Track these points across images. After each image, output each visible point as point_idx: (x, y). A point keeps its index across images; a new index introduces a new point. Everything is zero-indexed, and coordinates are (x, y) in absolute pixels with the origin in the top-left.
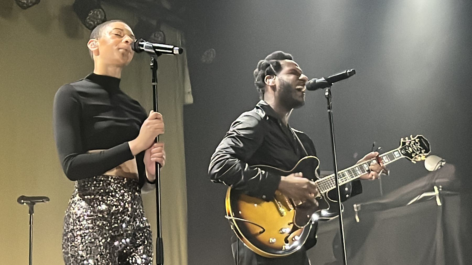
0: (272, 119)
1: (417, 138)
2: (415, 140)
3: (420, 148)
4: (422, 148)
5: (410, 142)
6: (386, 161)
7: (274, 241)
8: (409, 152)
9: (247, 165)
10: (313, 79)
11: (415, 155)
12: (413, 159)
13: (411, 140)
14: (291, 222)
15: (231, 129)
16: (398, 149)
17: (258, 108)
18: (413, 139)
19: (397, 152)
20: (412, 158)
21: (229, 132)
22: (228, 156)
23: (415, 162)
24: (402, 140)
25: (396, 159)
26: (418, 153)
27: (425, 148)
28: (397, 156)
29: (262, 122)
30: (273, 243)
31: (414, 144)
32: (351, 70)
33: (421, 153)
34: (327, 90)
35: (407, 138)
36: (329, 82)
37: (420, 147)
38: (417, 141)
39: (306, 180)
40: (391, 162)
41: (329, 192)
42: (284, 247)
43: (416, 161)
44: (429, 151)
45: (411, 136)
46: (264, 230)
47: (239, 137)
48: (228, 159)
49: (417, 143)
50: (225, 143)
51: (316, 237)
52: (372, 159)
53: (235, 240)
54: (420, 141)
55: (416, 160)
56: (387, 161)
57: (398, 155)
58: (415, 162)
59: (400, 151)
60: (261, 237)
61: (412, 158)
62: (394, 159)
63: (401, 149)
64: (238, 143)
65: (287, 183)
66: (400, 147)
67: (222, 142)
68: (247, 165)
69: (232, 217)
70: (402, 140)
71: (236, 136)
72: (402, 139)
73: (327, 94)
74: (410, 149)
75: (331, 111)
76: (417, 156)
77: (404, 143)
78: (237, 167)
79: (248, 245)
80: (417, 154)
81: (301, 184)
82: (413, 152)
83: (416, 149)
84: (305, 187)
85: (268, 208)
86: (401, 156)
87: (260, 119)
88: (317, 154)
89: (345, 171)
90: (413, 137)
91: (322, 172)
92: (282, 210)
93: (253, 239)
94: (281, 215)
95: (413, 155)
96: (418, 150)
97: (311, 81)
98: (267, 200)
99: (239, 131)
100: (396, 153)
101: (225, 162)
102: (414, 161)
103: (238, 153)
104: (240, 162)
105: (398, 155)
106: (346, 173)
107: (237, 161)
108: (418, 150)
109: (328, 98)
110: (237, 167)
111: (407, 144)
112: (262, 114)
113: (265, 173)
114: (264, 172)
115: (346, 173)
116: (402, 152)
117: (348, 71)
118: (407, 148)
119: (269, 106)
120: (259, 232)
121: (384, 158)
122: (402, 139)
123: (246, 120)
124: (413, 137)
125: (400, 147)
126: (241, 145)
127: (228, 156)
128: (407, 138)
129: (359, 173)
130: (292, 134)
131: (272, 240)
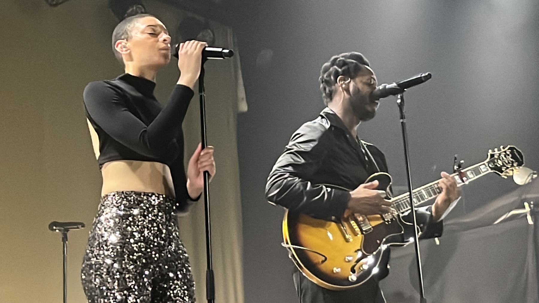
0: (337, 130)
1: (509, 149)
2: (505, 152)
3: (512, 161)
4: (514, 160)
5: (500, 154)
6: (472, 177)
7: (338, 270)
8: (499, 166)
10: (383, 85)
11: (506, 169)
12: (504, 174)
13: (501, 153)
14: (359, 248)
15: (291, 143)
16: (485, 162)
18: (503, 150)
19: (484, 166)
20: (502, 172)
21: (288, 147)
23: (506, 177)
24: (490, 152)
25: (482, 174)
26: (509, 166)
27: (517, 160)
28: (483, 170)
29: (326, 134)
30: (337, 273)
31: (505, 157)
32: (427, 74)
33: (512, 166)
34: (399, 96)
35: (496, 150)
36: (402, 88)
37: (511, 159)
38: (508, 153)
40: (476, 177)
42: (350, 277)
43: (507, 176)
44: (523, 163)
45: (502, 147)
46: (326, 259)
48: (286, 178)
49: (508, 155)
50: (284, 159)
52: (454, 174)
53: (296, 270)
55: (507, 174)
56: (471, 176)
57: (485, 169)
58: (506, 177)
59: (487, 164)
60: (324, 267)
61: (502, 172)
62: (480, 173)
63: (489, 163)
64: (298, 160)
66: (488, 160)
67: (280, 159)
69: (290, 245)
70: (490, 152)
71: (295, 151)
72: (490, 151)
73: (399, 101)
74: (500, 162)
75: (405, 121)
76: (507, 170)
77: (492, 156)
78: (297, 187)
79: (307, 273)
80: (508, 168)
82: (504, 166)
83: (507, 162)
86: (488, 170)
88: (389, 169)
89: (422, 189)
90: (504, 148)
94: (347, 241)
95: (503, 169)
96: (509, 163)
97: (381, 87)
99: (300, 145)
100: (482, 167)
101: (283, 182)
102: (505, 175)
103: (297, 170)
104: (301, 181)
105: (485, 169)
106: (424, 192)
107: (297, 180)
108: (509, 163)
109: (401, 106)
110: (297, 187)
111: (496, 157)
115: (424, 192)
116: (490, 165)
117: (423, 75)
118: (496, 161)
120: (320, 261)
121: (468, 173)
122: (490, 151)
124: (504, 148)
125: (488, 160)
128: (496, 150)
130: (358, 146)
131: (336, 270)
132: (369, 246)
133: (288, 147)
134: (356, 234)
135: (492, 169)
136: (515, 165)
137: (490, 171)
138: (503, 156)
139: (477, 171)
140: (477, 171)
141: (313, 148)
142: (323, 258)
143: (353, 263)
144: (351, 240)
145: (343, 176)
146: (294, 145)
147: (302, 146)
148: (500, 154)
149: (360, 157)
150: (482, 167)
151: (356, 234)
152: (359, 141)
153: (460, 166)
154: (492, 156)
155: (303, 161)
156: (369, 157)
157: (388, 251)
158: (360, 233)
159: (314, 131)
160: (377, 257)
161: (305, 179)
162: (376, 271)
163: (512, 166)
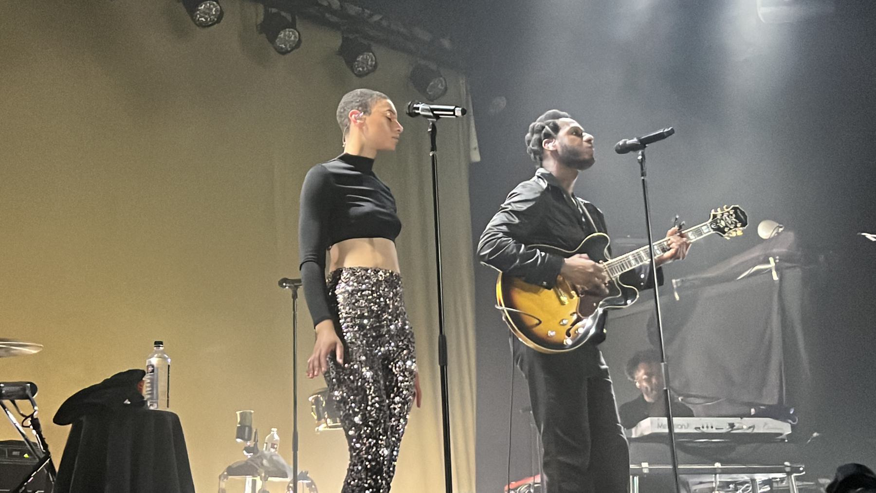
0: (555, 190)
5: (723, 214)
6: (693, 238)
9: (523, 246)
13: (724, 213)
15: (506, 202)
17: (539, 177)
20: (724, 233)
21: (503, 205)
22: (501, 235)
24: (713, 212)
29: (544, 192)
33: (736, 227)
35: (719, 209)
39: (592, 262)
41: (621, 276)
47: (516, 213)
50: (498, 218)
51: (605, 331)
54: (735, 213)
57: (707, 230)
61: (724, 233)
63: (711, 224)
65: (571, 267)
66: (710, 220)
67: (494, 218)
68: (523, 246)
70: (713, 212)
77: (715, 216)
78: (510, 248)
81: (585, 267)
84: (591, 270)
85: (549, 295)
87: (541, 190)
91: (614, 251)
92: (564, 298)
93: (528, 332)
95: (726, 230)
98: (548, 288)
100: (704, 228)
107: (511, 241)
110: (510, 248)
111: (719, 217)
112: (544, 185)
113: (545, 256)
114: (543, 254)
119: (550, 174)
123: (527, 191)
125: (710, 220)
126: (517, 221)
127: (501, 235)
128: (719, 209)
129: (658, 252)
132: (584, 310)
133: (503, 205)
134: (571, 297)
135: (714, 230)
136: (739, 225)
137: (712, 232)
138: (725, 215)
139: (699, 232)
140: (699, 232)
141: (529, 209)
142: (537, 322)
143: (569, 327)
144: (567, 303)
145: (559, 236)
146: (509, 204)
147: (518, 205)
148: (723, 214)
149: (574, 216)
150: (704, 228)
151: (571, 297)
152: (575, 199)
153: (680, 227)
154: (715, 216)
155: (517, 221)
156: (586, 218)
157: (605, 312)
158: (576, 296)
159: (530, 191)
160: (594, 318)
161: (519, 241)
162: (592, 331)
163: (736, 227)
